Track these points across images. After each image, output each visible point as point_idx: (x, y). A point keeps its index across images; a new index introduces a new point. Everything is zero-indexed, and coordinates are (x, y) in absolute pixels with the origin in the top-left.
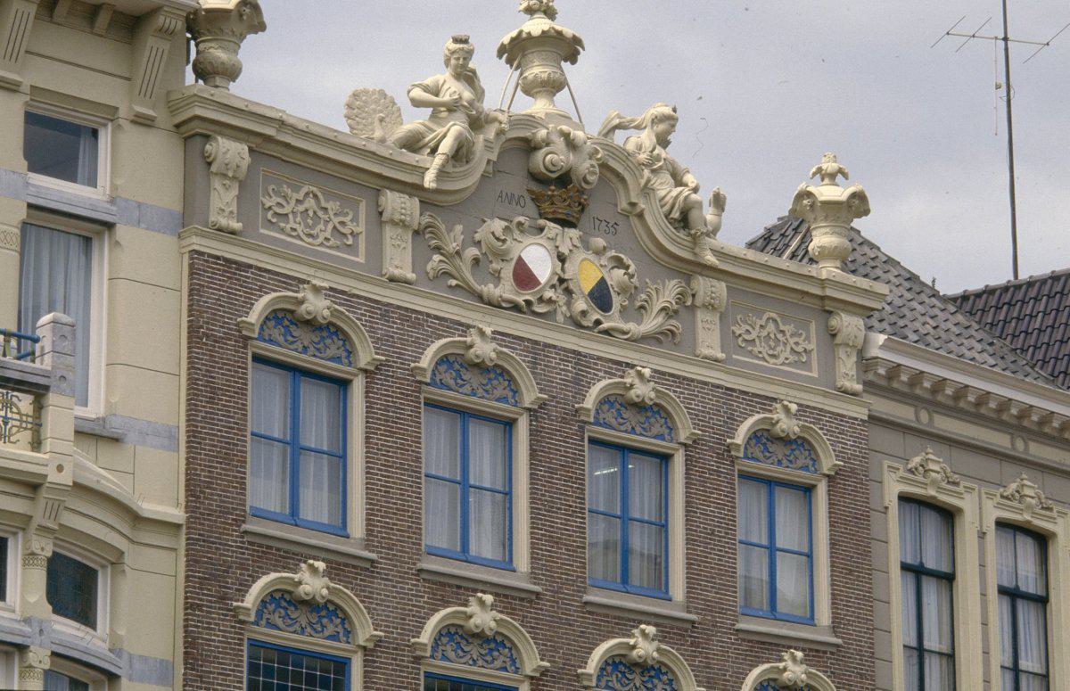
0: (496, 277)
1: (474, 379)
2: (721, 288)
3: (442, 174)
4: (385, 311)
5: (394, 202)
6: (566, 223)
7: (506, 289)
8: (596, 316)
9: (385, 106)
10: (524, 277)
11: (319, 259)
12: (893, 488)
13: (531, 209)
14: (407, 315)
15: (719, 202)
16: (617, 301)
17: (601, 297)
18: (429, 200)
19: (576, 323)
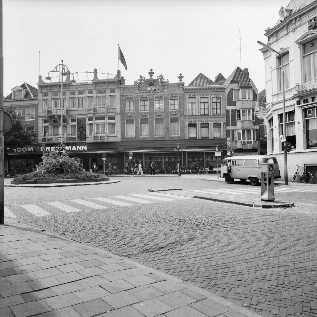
0: (145, 91)
1: (144, 98)
2: (167, 87)
3: (138, 86)
4: (136, 96)
5: (136, 88)
6: (151, 86)
7: (146, 92)
8: (154, 91)
9: (137, 81)
10: (147, 90)
11: (127, 94)
12: (187, 97)
13: (149, 85)
14: (137, 95)
15: (168, 80)
16: (156, 90)
17: (155, 90)
18: (138, 87)
19: (153, 92)
